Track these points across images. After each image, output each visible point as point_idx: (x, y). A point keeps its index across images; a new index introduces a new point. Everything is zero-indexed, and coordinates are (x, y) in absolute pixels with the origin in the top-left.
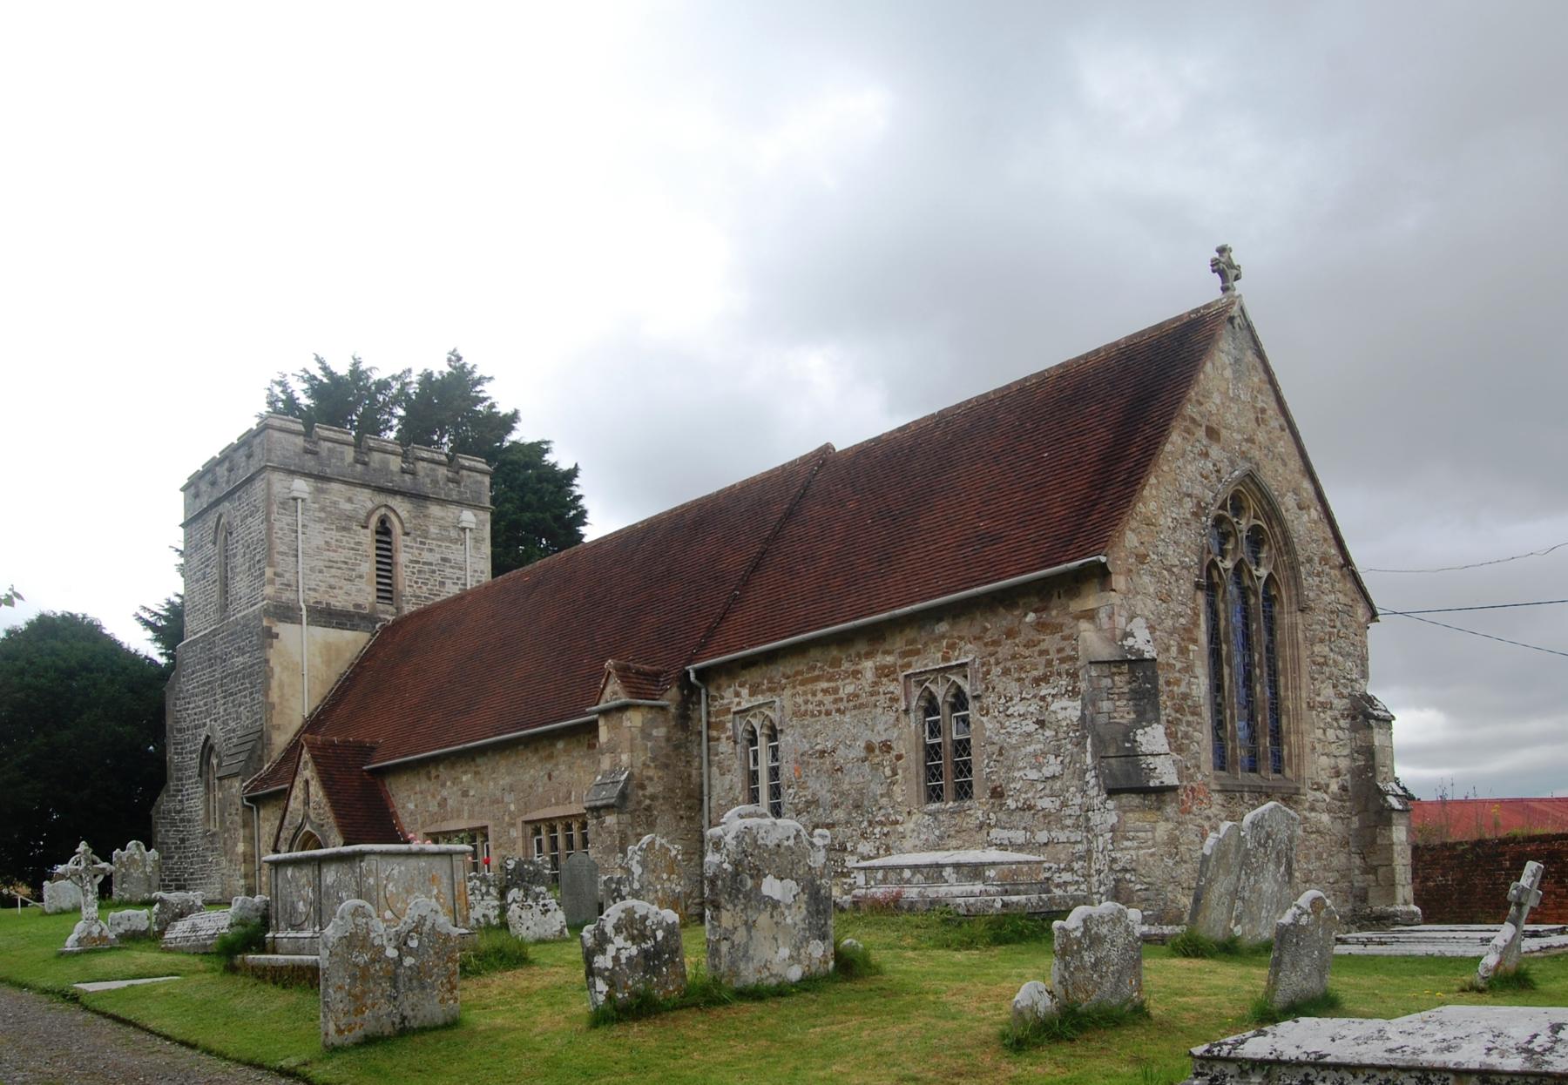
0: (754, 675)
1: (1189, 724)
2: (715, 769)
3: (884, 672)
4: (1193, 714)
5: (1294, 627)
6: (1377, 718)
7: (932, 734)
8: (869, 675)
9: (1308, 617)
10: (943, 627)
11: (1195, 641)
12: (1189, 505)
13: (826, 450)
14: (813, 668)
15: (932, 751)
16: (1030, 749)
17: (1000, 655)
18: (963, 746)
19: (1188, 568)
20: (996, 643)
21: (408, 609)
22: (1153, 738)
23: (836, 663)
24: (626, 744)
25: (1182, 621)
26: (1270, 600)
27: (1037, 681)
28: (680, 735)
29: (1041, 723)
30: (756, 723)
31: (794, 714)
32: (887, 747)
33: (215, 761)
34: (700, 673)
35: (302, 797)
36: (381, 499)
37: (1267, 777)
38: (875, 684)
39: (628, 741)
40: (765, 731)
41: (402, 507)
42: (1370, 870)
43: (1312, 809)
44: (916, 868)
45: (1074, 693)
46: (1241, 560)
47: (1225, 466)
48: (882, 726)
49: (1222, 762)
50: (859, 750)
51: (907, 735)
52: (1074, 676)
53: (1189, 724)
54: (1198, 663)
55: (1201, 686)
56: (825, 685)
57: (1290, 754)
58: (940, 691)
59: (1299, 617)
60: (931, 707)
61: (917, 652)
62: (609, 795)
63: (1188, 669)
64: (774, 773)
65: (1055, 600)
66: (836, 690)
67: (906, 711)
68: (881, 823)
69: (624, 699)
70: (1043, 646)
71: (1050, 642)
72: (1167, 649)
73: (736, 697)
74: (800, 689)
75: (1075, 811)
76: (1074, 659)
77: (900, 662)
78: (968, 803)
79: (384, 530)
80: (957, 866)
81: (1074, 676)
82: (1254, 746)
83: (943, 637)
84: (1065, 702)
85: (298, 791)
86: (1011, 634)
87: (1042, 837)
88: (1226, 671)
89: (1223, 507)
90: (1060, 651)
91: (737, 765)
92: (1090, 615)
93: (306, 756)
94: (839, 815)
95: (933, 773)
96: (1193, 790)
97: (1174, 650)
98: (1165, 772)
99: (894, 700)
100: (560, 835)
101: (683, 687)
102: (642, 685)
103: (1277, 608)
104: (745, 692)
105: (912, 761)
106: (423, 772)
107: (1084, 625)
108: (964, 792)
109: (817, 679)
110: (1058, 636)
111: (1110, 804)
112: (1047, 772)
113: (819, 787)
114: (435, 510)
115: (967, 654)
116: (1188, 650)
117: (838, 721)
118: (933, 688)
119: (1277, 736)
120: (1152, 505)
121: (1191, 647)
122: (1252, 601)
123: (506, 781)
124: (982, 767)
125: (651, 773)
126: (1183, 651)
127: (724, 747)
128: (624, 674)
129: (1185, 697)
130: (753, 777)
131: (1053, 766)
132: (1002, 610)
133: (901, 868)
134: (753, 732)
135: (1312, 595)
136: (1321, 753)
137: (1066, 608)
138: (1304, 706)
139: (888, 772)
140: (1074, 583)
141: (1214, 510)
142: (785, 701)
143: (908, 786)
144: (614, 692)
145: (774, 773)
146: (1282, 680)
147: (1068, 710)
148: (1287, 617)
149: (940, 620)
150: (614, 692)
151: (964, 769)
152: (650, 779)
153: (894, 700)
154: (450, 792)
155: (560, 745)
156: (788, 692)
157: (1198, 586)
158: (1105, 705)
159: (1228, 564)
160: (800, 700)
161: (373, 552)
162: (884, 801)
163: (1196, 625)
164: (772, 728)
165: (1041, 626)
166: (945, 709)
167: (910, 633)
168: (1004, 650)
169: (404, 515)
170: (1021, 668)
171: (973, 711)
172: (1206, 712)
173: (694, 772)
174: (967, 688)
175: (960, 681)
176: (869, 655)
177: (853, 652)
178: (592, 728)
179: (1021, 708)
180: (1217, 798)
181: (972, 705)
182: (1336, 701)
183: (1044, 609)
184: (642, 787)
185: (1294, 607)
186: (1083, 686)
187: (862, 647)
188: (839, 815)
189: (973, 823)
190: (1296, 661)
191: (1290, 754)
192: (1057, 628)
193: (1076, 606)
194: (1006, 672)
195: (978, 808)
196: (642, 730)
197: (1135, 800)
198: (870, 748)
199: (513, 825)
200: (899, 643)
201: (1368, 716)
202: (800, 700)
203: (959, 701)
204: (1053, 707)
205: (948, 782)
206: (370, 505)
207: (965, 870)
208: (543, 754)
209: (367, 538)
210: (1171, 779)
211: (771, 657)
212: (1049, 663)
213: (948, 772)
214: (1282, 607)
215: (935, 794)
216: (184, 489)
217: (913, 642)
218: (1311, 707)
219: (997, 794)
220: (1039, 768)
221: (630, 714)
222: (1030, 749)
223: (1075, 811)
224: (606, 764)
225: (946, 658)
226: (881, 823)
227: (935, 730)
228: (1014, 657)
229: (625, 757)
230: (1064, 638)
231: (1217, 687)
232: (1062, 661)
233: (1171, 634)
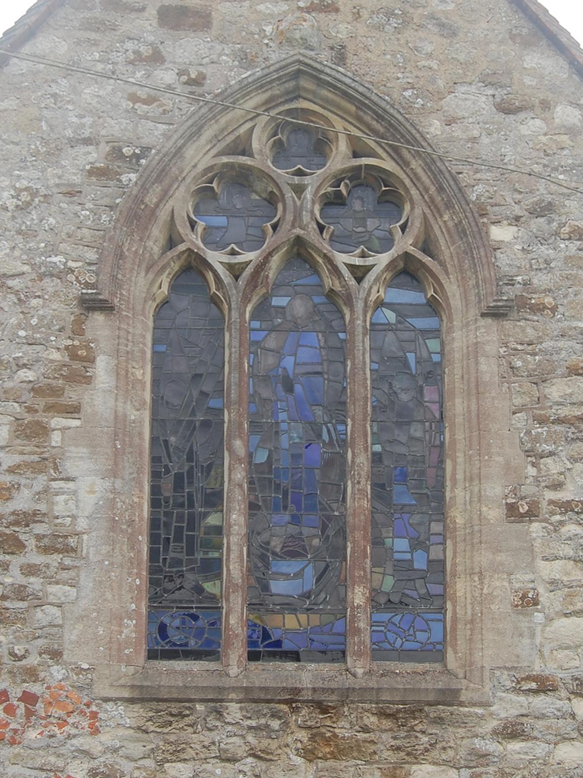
1: (30, 570)
4: (46, 550)
5: (475, 351)
9: (524, 328)
11: (73, 410)
19: (61, 274)
25: (29, 375)
43: (512, 731)
53: (30, 570)
57: (455, 619)
59: (489, 334)
63: (48, 464)
96: (29, 698)
121: (57, 422)
129: (27, 519)
135: (540, 280)
138: (494, 514)
180: (121, 718)
185: (474, 312)
190: (479, 422)
191: (455, 619)
214: (450, 319)
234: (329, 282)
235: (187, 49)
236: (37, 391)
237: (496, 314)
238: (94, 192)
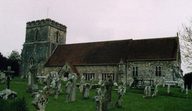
15: (156, 72)
27: (169, 67)
29: (169, 71)
32: (151, 71)
42: (136, 78)
45: (172, 69)
48: (151, 69)
50: (148, 71)
58: (158, 67)
64: (137, 72)
69: (123, 63)
71: (170, 64)
86: (166, 63)
87: (168, 80)
92: (174, 63)
104: (133, 64)
108: (160, 75)
124: (162, 73)
130: (134, 72)
140: (173, 60)
142: (139, 65)
145: (137, 72)
151: (161, 74)
174: (161, 67)
188: (145, 76)
192: (171, 63)
193: (172, 62)
194: (165, 66)
198: (149, 71)
200: (154, 62)
203: (160, 68)
215: (157, 75)
227: (157, 70)
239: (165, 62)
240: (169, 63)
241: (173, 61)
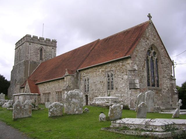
0: (86, 71)
2: (80, 85)
3: (102, 71)
6: (173, 79)
7: (109, 80)
8: (101, 71)
10: (110, 65)
11: (145, 68)
12: (144, 48)
13: (99, 40)
14: (93, 70)
15: (109, 83)
16: (121, 83)
17: (117, 69)
18: (112, 82)
20: (117, 67)
21: (44, 61)
22: (137, 81)
23: (96, 70)
24: (68, 81)
25: (143, 65)
26: (157, 62)
27: (122, 73)
28: (76, 79)
29: (122, 79)
30: (86, 78)
31: (91, 77)
33: (17, 82)
34: (79, 71)
35: (26, 88)
36: (41, 46)
37: (156, 87)
38: (102, 73)
39: (68, 80)
40: (87, 79)
41: (44, 47)
43: (163, 92)
44: (101, 99)
45: (127, 75)
46: (152, 56)
47: (149, 43)
49: (149, 85)
51: (105, 80)
52: (127, 72)
54: (145, 71)
55: (145, 74)
56: (95, 73)
58: (109, 74)
59: (161, 65)
60: (109, 77)
61: (107, 68)
62: (65, 88)
63: (143, 72)
65: (124, 62)
66: (96, 74)
67: (105, 77)
68: (101, 93)
69: (68, 74)
70: (123, 68)
71: (124, 67)
72: (140, 68)
73: (83, 74)
74: (92, 73)
75: (127, 91)
76: (126, 70)
77: (104, 70)
78: (113, 90)
79: (41, 50)
80: (106, 99)
81: (127, 72)
82: (153, 83)
83: (110, 66)
84: (125, 76)
85: (26, 87)
86: (119, 66)
88: (150, 72)
89: (149, 49)
90: (125, 69)
91: (83, 84)
93: (27, 82)
94: (96, 91)
95: (109, 86)
96: (144, 89)
97: (141, 69)
98: (138, 86)
99: (104, 75)
100: (60, 94)
101: (76, 73)
102: (71, 72)
103: (158, 63)
105: (106, 84)
106: (43, 85)
107: (128, 65)
109: (94, 72)
110: (125, 66)
111: (130, 90)
112: (123, 86)
113: (93, 87)
114: (49, 47)
115: (113, 69)
116: (143, 69)
117: (95, 78)
118: (109, 73)
119: (158, 81)
120: (138, 48)
121: (144, 68)
122: (154, 62)
123: (53, 86)
125: (71, 85)
126: (143, 69)
127: (82, 81)
128: (68, 71)
129: (143, 75)
130: (85, 86)
131: (124, 85)
132: (117, 63)
133: (99, 99)
134: (86, 79)
135: (163, 61)
136: (165, 84)
137: (125, 63)
139: (103, 85)
141: (147, 49)
143: (105, 88)
144: (67, 73)
146: (159, 73)
147: (126, 77)
148: (159, 64)
149: (110, 64)
150: (67, 73)
151: (112, 85)
152: (71, 86)
153: (104, 75)
154: (46, 87)
155: (60, 81)
156: (90, 74)
157: (145, 60)
158: (130, 77)
159: (150, 57)
160: (92, 75)
161: (40, 53)
162: (102, 90)
163: (145, 65)
164: (88, 79)
165: (123, 65)
166: (110, 76)
167: (106, 66)
168: (118, 68)
169: (45, 48)
170: (120, 71)
171: (113, 77)
172: (146, 78)
173: (78, 85)
174: (113, 74)
175: (112, 72)
176: (101, 69)
177: (98, 68)
178: (64, 78)
179: (120, 76)
181: (114, 76)
182: (167, 77)
183: (123, 63)
184: (70, 87)
185: (160, 63)
186: (128, 74)
187: (100, 67)
188: (96, 91)
189: (113, 93)
194: (118, 71)
195: (114, 91)
196: (70, 79)
197: (134, 90)
198: (100, 82)
199: (54, 92)
201: (172, 79)
202: (92, 75)
204: (124, 76)
205: (110, 87)
206: (40, 47)
207: (107, 99)
208: (58, 82)
209: (39, 51)
210: (139, 87)
211: (88, 68)
212: (123, 70)
213: (110, 86)
215: (109, 89)
216: (15, 44)
217: (106, 67)
218: (163, 77)
219: (117, 89)
220: (122, 85)
221: (68, 76)
222: (121, 83)
223: (127, 91)
224: (65, 84)
225: (110, 69)
226: (101, 93)
228: (119, 69)
229: (68, 83)
230: (125, 67)
231: (148, 74)
232: (125, 70)
233: (141, 67)
234: (153, 59)
235: (148, 41)
236: (143, 66)
237: (162, 63)
238: (144, 51)
239: (117, 64)
240: (123, 65)
241: (127, 61)
